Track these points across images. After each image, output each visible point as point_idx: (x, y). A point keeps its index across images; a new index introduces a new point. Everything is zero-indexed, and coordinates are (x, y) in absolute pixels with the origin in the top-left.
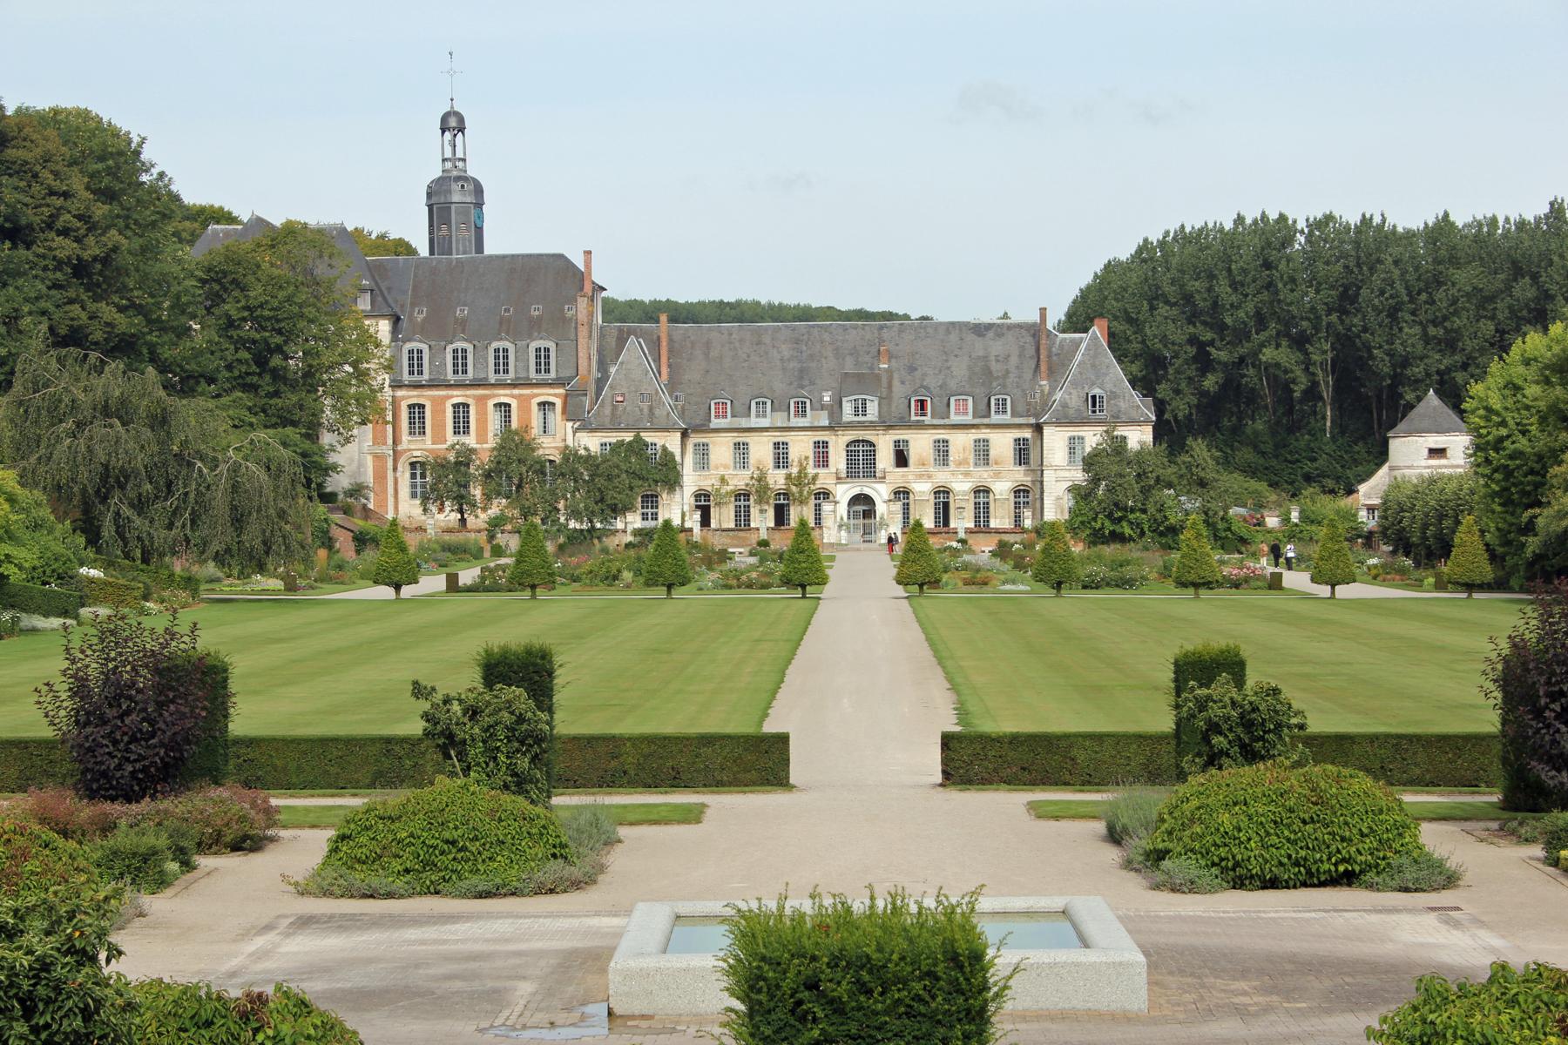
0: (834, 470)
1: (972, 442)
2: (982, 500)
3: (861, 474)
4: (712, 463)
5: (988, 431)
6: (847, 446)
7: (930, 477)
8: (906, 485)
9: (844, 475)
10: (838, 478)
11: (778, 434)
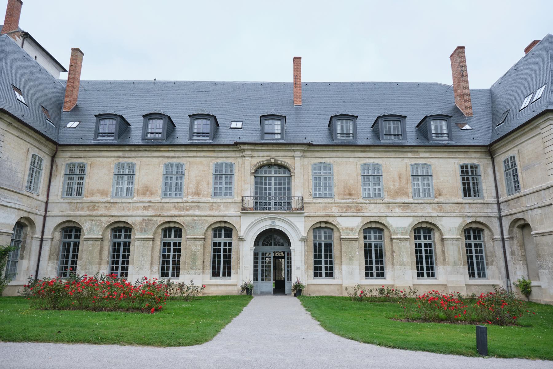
0: (240, 199)
1: (409, 168)
2: (423, 242)
3: (272, 205)
4: (85, 192)
5: (427, 155)
6: (256, 171)
7: (359, 210)
8: (330, 220)
9: (250, 204)
10: (244, 209)
11: (172, 154)
